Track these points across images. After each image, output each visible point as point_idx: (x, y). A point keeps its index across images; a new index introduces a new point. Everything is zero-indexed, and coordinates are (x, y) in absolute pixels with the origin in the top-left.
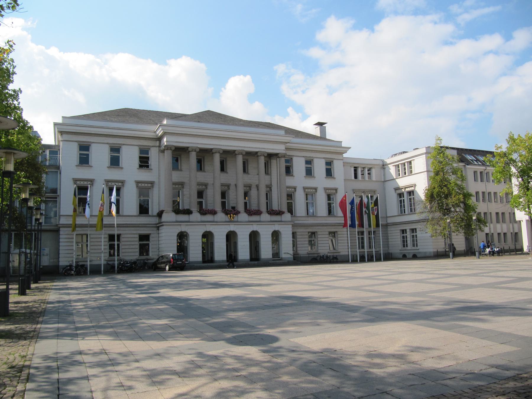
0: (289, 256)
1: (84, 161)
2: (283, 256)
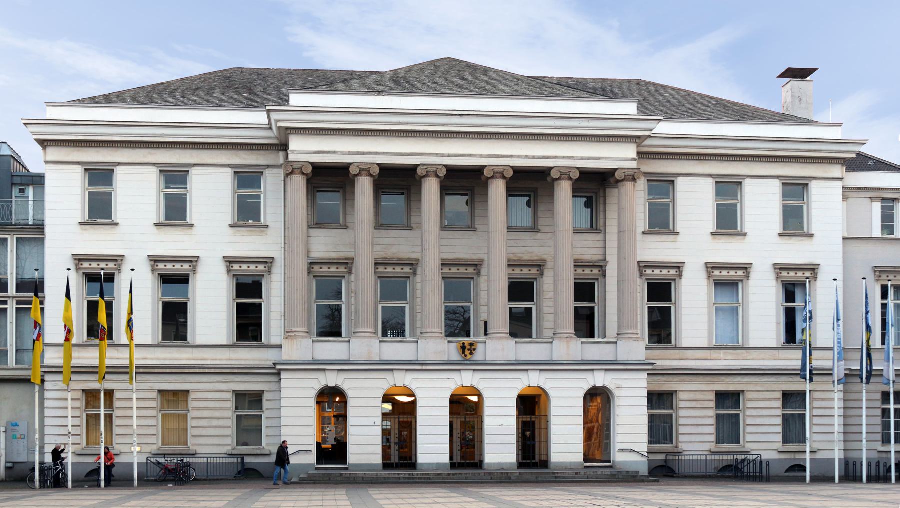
0: (638, 458)
1: (100, 210)
2: (618, 457)
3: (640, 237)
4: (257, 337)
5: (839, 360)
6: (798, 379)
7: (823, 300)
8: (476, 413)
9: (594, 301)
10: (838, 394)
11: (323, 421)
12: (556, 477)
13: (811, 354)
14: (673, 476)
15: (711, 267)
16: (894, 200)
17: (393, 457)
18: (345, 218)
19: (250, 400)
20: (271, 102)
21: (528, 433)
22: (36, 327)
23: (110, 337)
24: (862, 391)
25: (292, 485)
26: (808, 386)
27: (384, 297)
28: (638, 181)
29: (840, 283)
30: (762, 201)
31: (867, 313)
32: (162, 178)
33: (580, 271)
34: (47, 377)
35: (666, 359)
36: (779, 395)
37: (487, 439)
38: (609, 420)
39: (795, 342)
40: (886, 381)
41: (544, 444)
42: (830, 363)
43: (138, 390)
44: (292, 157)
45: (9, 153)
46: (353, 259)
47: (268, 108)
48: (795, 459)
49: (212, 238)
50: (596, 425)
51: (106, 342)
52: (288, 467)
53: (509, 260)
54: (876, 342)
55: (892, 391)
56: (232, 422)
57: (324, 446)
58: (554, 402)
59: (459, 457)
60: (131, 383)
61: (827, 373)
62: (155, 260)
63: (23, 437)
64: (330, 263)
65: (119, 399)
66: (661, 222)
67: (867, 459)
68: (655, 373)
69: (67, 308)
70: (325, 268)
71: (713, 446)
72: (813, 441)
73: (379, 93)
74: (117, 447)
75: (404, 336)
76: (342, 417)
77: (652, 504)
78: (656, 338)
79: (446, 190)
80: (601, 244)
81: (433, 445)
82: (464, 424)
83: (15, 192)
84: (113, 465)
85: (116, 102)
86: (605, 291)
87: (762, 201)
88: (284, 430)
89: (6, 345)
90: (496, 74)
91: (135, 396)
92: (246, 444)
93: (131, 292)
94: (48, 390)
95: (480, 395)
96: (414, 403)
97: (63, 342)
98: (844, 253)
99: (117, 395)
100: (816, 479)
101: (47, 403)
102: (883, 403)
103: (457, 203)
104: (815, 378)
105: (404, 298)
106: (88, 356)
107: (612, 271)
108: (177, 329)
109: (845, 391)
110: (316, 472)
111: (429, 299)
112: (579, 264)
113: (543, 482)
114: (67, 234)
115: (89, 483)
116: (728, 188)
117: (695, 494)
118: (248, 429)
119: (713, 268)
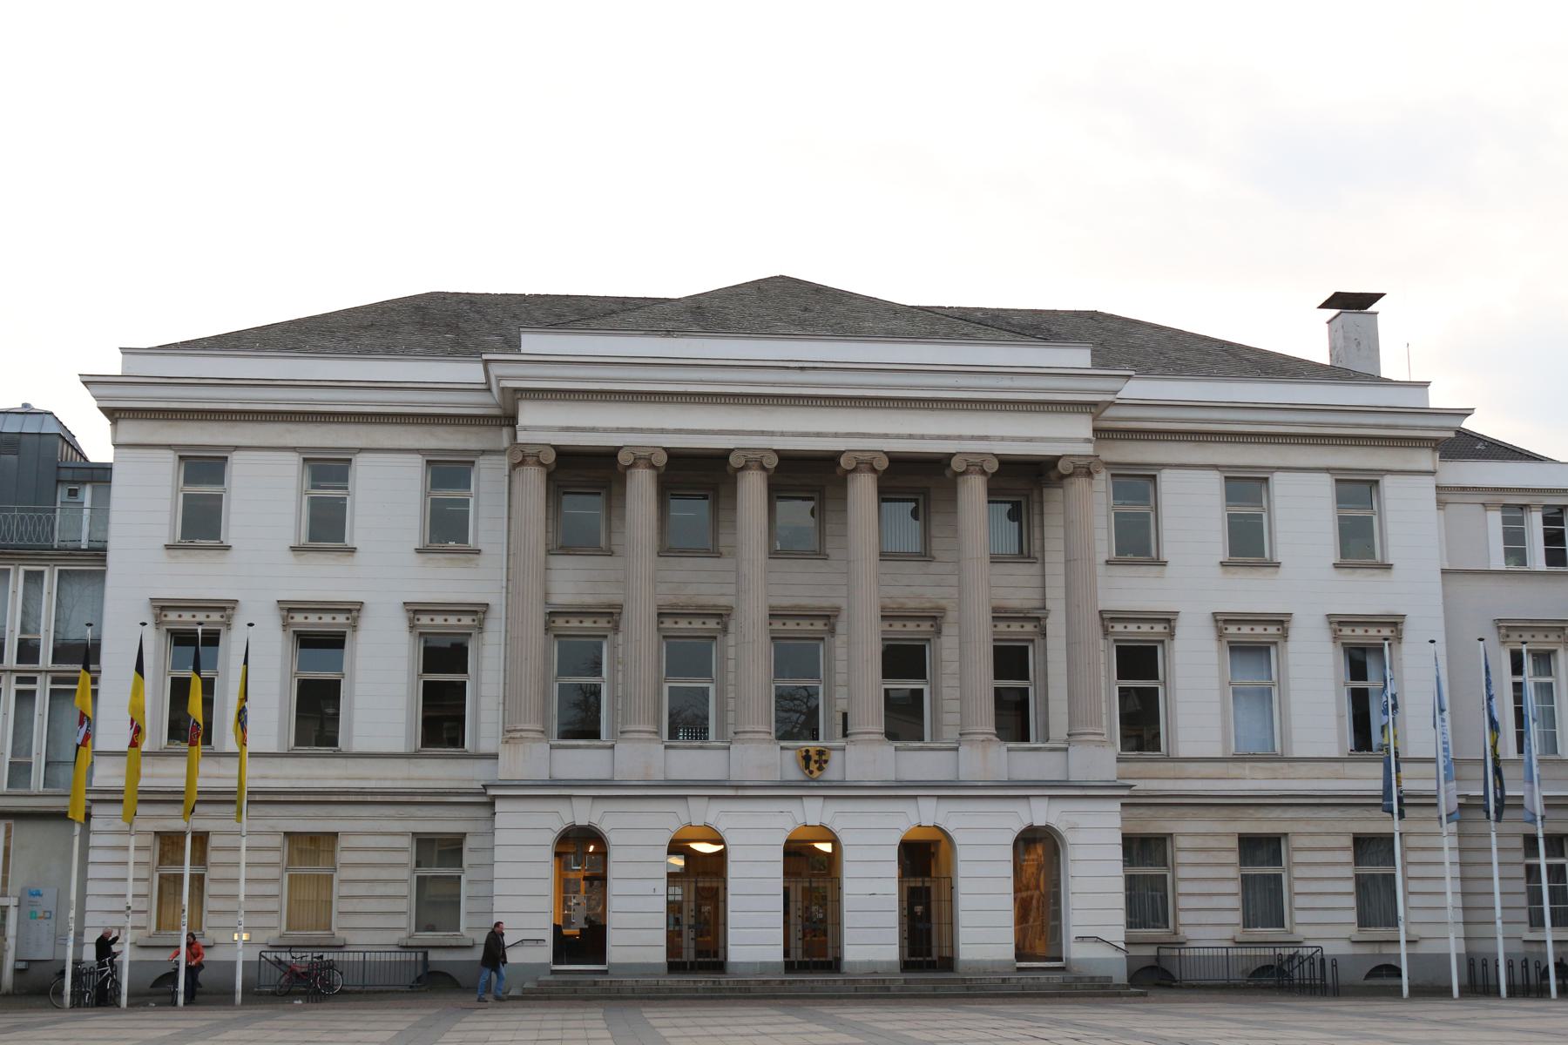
0: (1110, 953)
1: (201, 525)
2: (1075, 952)
3: (1101, 569)
4: (457, 740)
5: (1447, 780)
6: (1378, 813)
7: (1415, 674)
8: (829, 874)
9: (1027, 678)
10: (1447, 840)
11: (565, 887)
12: (968, 988)
13: (1398, 770)
14: (1170, 987)
15: (1222, 621)
16: (1522, 507)
17: (685, 952)
18: (609, 538)
19: (441, 851)
20: (490, 347)
21: (918, 909)
22: (81, 723)
23: (207, 740)
24: (1489, 835)
25: (510, 1003)
26: (1396, 826)
27: (673, 671)
28: (1096, 476)
29: (1440, 647)
30: (1303, 509)
31: (1490, 698)
32: (307, 471)
33: (1002, 626)
34: (96, 810)
35: (1151, 778)
36: (1348, 842)
37: (848, 919)
38: (1058, 885)
39: (1370, 749)
40: (1530, 817)
41: (945, 929)
42: (1432, 785)
43: (249, 833)
44: (522, 437)
45: (55, 430)
46: (621, 606)
47: (485, 357)
48: (1382, 955)
49: (387, 572)
50: (1036, 893)
51: (200, 748)
52: (503, 970)
53: (883, 609)
54: (1509, 749)
55: (1540, 834)
56: (408, 890)
57: (566, 932)
58: (962, 854)
59: (800, 952)
60: (239, 820)
61: (1428, 802)
62: (289, 609)
63: (47, 916)
64: (582, 613)
65: (217, 849)
66: (1137, 544)
67: (1506, 954)
68: (1133, 803)
69: (137, 691)
70: (574, 623)
71: (1238, 932)
72: (1409, 923)
73: (669, 333)
74: (209, 933)
75: (706, 738)
76: (598, 880)
77: (1137, 1037)
78: (1133, 742)
79: (777, 490)
80: (1037, 582)
81: (755, 931)
82: (808, 893)
83: (62, 493)
84: (200, 966)
85: (236, 347)
86: (1046, 662)
87: (1303, 509)
88: (499, 904)
89: (29, 754)
90: (858, 303)
91: (244, 843)
92: (431, 928)
93: (246, 662)
94: (96, 832)
95: (835, 842)
96: (721, 856)
97: (126, 748)
98: (1445, 597)
99: (214, 841)
100: (1418, 991)
101: (93, 856)
102: (1527, 855)
103: (797, 513)
104: (1408, 812)
105: (705, 672)
106: (167, 774)
107: (1056, 626)
108: (322, 727)
109: (1461, 835)
110: (551, 978)
111: (748, 674)
112: (1001, 615)
113: (946, 996)
114: (143, 564)
115: (158, 999)
116: (1246, 488)
117: (1209, 1018)
118: (437, 904)
119: (1226, 621)
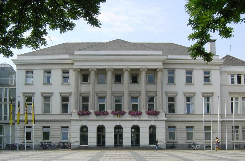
9: (154, 102)
35: (172, 117)
49: (57, 87)
62: (42, 93)
66: (171, 80)
73: (98, 50)
